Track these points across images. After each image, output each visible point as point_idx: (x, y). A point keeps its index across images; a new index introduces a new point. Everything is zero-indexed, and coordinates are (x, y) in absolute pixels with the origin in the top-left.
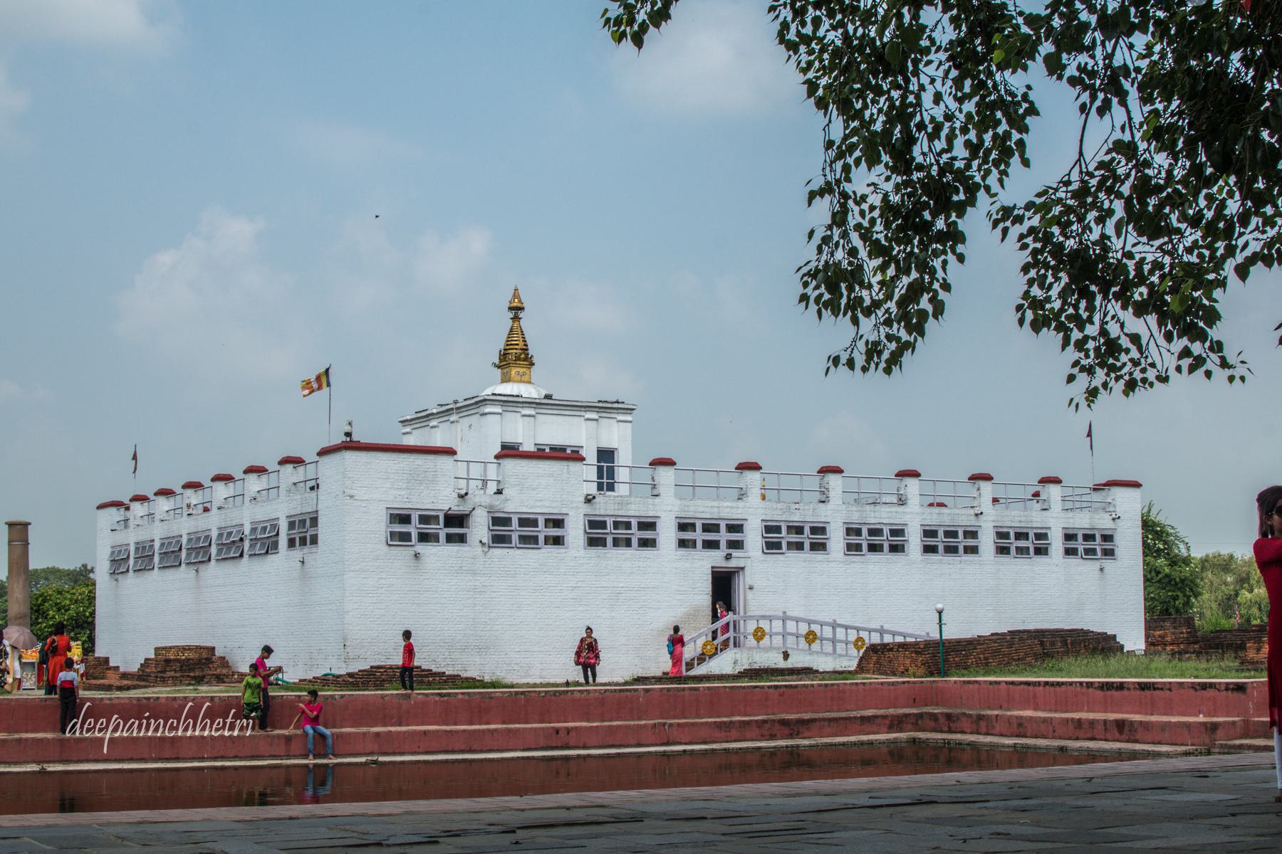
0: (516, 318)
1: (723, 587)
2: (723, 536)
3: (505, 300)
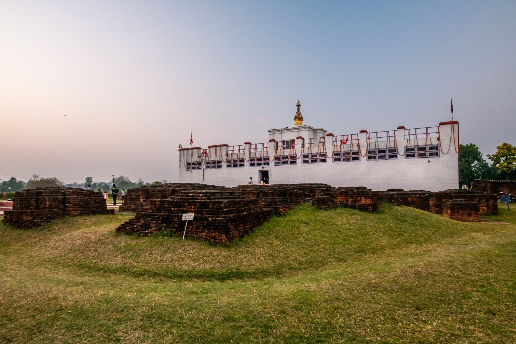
0: (299, 109)
1: (265, 175)
2: (262, 162)
3: (296, 104)
